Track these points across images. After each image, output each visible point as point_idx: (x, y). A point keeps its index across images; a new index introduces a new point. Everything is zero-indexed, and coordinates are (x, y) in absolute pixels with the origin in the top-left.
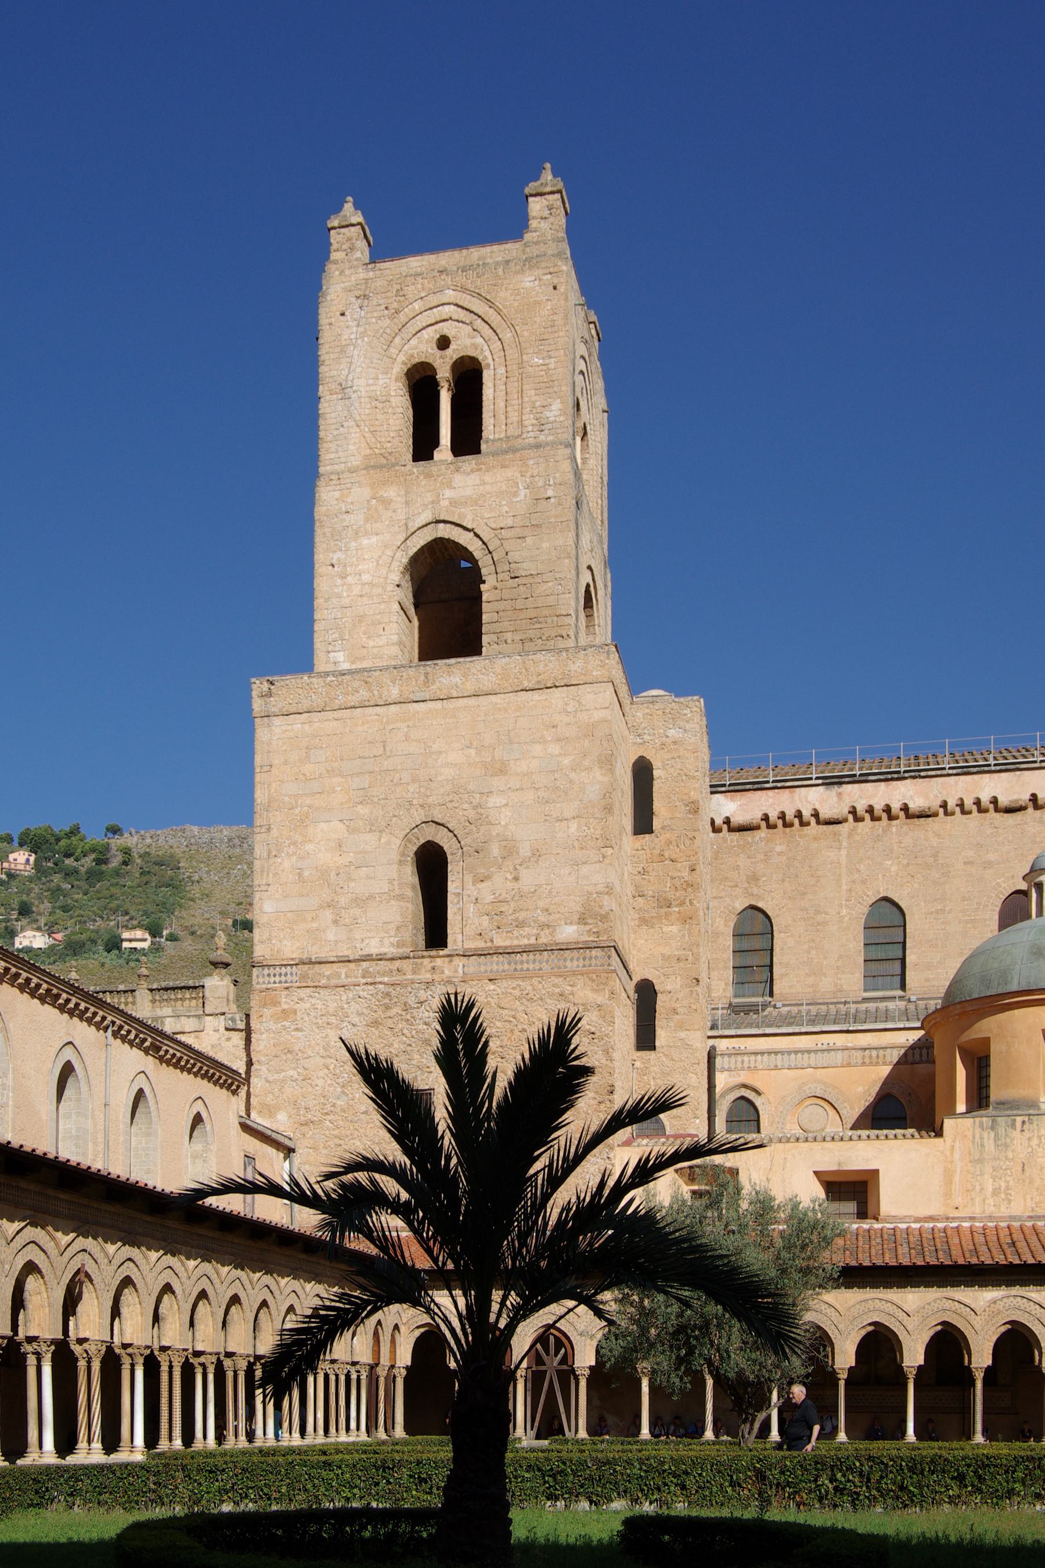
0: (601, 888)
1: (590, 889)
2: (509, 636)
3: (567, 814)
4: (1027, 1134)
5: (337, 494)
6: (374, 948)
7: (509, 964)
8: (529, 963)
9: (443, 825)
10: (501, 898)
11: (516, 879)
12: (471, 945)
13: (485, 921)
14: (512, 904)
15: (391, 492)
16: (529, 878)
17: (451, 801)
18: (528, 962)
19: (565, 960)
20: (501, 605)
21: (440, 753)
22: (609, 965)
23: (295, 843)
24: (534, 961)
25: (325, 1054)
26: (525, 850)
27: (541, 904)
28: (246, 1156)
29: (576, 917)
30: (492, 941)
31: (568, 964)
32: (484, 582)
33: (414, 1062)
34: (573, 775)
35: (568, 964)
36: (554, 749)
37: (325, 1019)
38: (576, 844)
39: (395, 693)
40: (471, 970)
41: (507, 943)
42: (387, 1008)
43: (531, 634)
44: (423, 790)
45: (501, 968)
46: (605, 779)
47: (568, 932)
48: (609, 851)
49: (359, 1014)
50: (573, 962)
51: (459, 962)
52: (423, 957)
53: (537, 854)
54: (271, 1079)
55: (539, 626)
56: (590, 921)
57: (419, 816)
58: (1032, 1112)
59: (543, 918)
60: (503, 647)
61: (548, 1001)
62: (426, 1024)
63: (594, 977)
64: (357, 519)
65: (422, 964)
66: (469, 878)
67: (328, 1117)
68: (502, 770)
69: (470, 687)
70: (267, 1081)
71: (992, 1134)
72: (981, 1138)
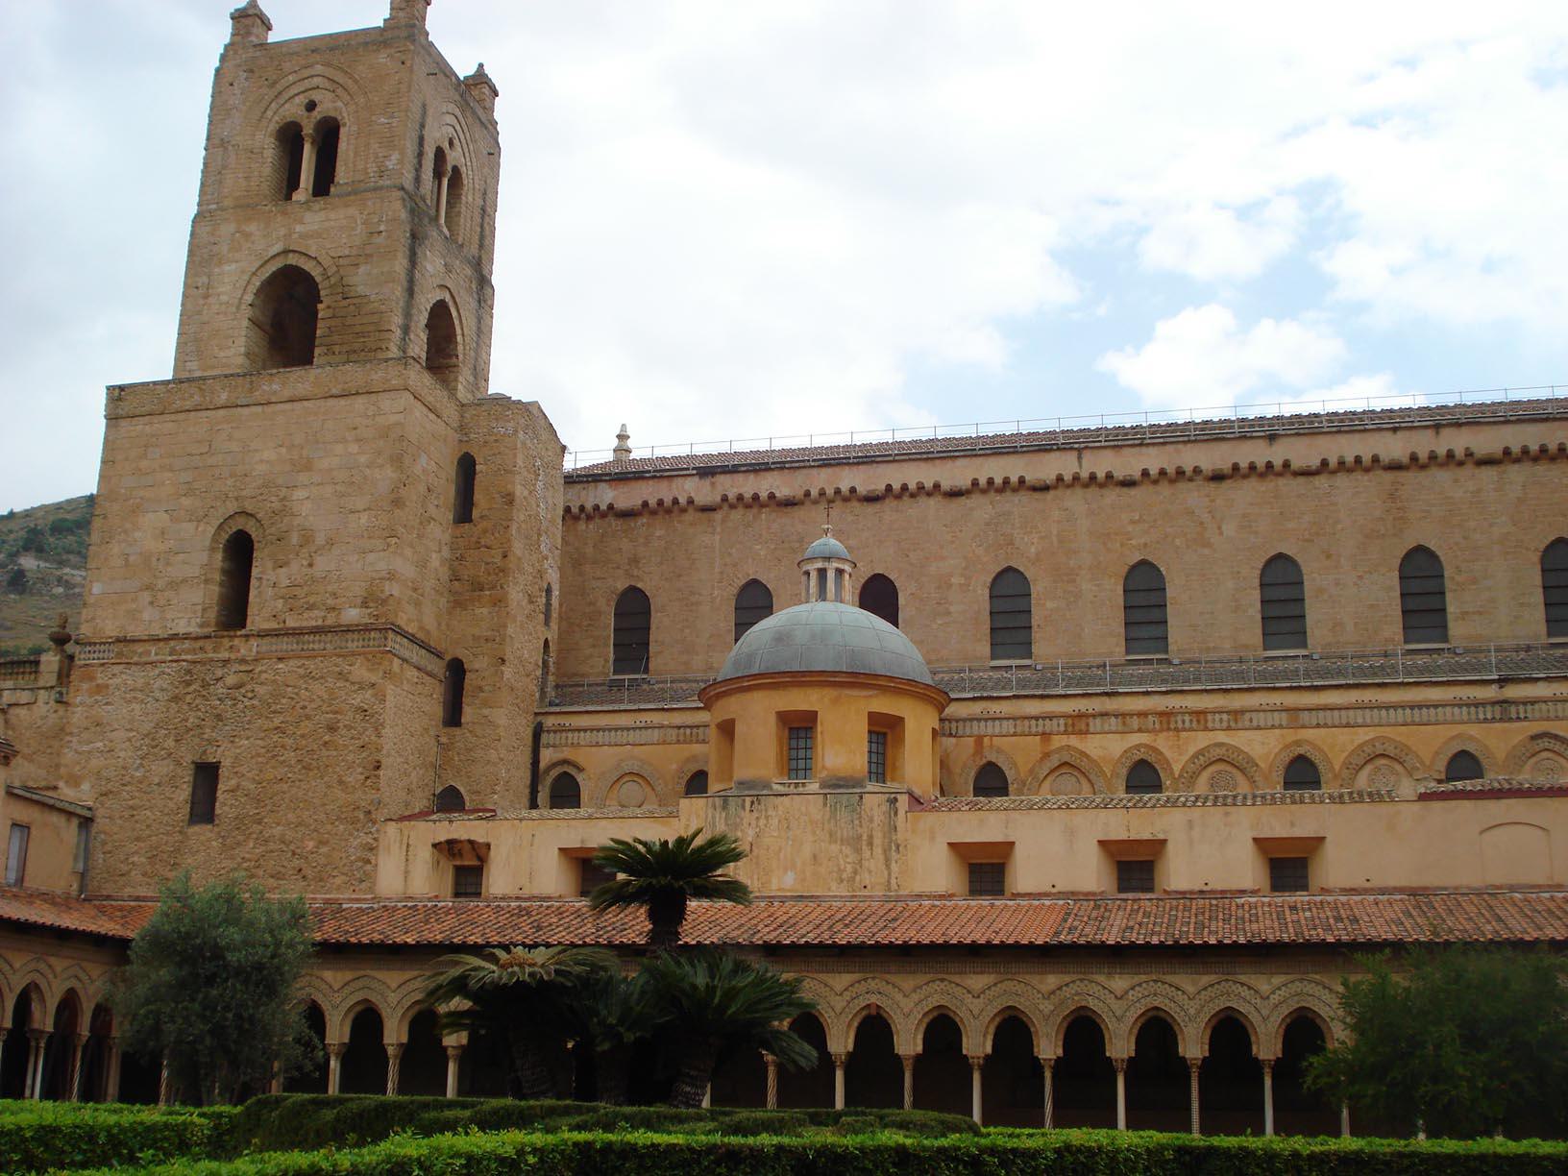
0: (384, 574)
1: (374, 575)
2: (337, 349)
3: (360, 506)
4: (755, 814)
5: (208, 229)
6: (181, 628)
7: (298, 643)
8: (315, 644)
9: (251, 515)
10: (296, 583)
11: (311, 565)
12: (266, 626)
13: (280, 603)
14: (306, 588)
15: (252, 228)
16: (322, 564)
17: (261, 494)
18: (313, 642)
19: (347, 641)
20: (333, 323)
21: (256, 451)
22: (385, 646)
23: (125, 532)
24: (320, 641)
25: (129, 727)
26: (320, 539)
27: (330, 589)
28: (14, 825)
29: (359, 601)
30: (284, 622)
31: (350, 644)
32: (321, 302)
33: (206, 736)
34: (368, 472)
35: (350, 644)
36: (354, 448)
37: (133, 694)
38: (365, 534)
39: (224, 397)
40: (264, 649)
41: (297, 625)
42: (188, 684)
43: (356, 346)
44: (238, 484)
45: (290, 647)
46: (394, 475)
47: (352, 615)
48: (394, 540)
49: (162, 690)
50: (353, 644)
51: (254, 642)
52: (223, 637)
53: (331, 543)
54: (80, 750)
55: (362, 340)
56: (371, 605)
57: (232, 507)
58: (765, 792)
59: (330, 602)
60: (330, 358)
61: (330, 680)
62: (219, 699)
63: (370, 657)
64: (224, 249)
65: (221, 643)
66: (270, 564)
67: (127, 788)
68: (308, 467)
69: (287, 394)
70: (76, 752)
71: (724, 815)
72: (714, 817)
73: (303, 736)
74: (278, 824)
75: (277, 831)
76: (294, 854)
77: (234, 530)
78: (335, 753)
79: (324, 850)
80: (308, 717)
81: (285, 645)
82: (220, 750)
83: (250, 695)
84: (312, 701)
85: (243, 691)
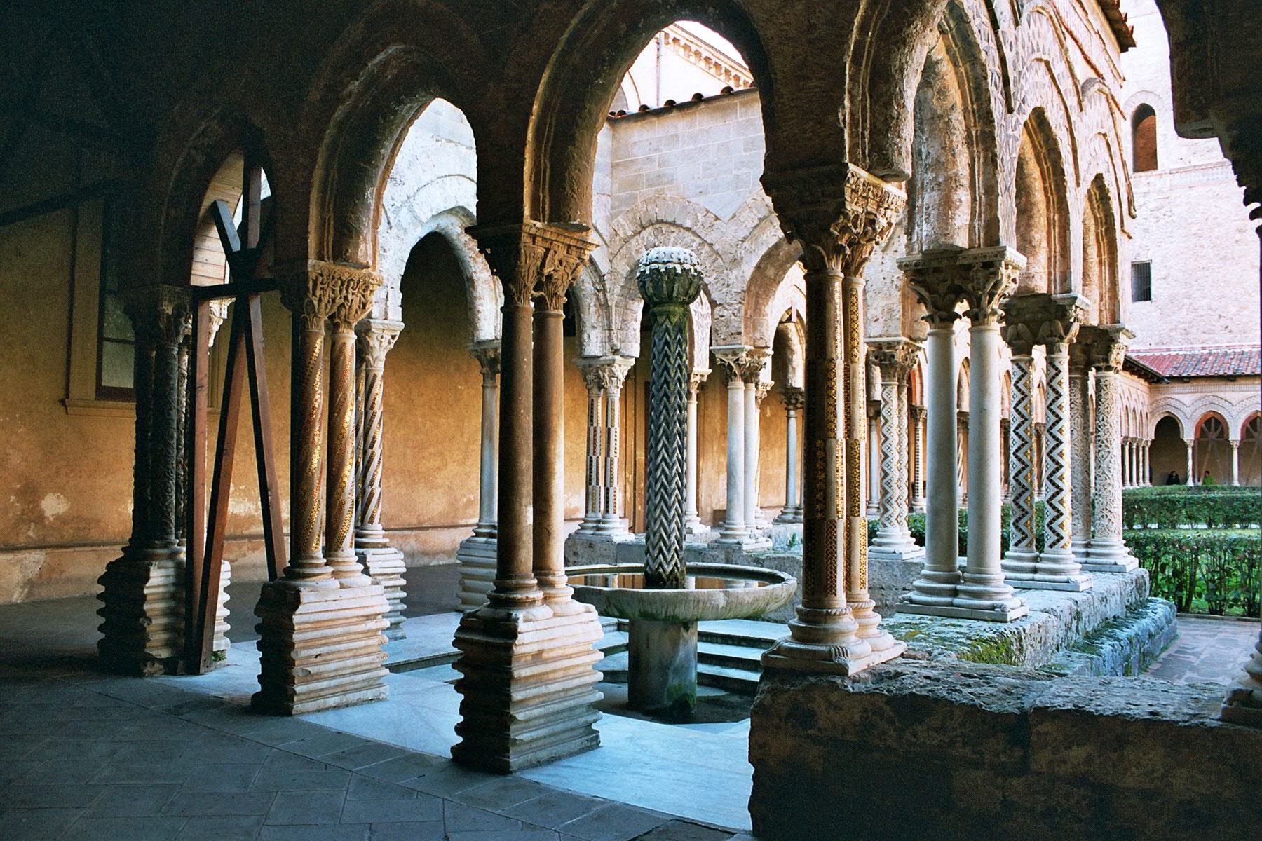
7: (1203, 176)
9: (1152, 92)
18: (1213, 174)
24: (1222, 173)
51: (1168, 178)
62: (1144, 219)
73: (1217, 238)
74: (1204, 298)
75: (1204, 302)
76: (1220, 316)
77: (1138, 104)
78: (1246, 247)
79: (1246, 312)
80: (1219, 225)
81: (1193, 177)
82: (1150, 252)
83: (1169, 214)
84: (1222, 213)
85: (1163, 211)
